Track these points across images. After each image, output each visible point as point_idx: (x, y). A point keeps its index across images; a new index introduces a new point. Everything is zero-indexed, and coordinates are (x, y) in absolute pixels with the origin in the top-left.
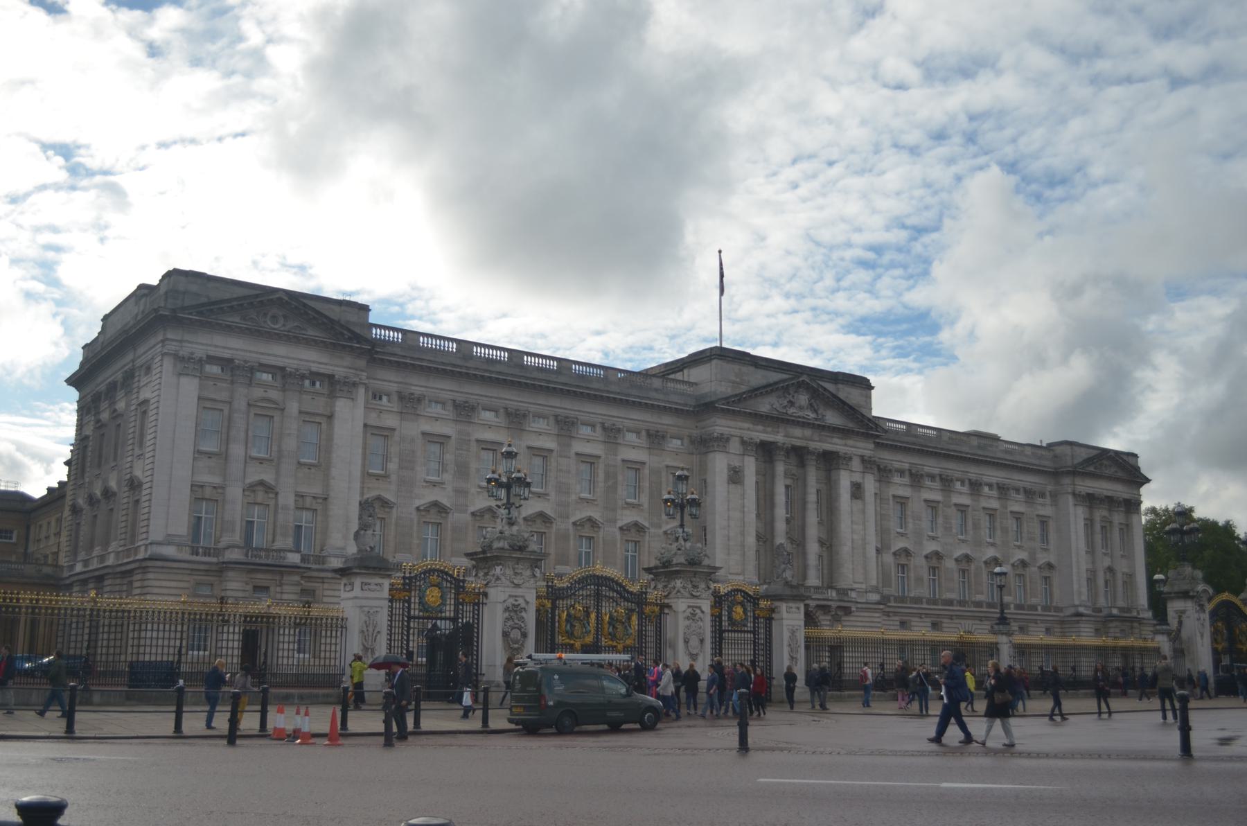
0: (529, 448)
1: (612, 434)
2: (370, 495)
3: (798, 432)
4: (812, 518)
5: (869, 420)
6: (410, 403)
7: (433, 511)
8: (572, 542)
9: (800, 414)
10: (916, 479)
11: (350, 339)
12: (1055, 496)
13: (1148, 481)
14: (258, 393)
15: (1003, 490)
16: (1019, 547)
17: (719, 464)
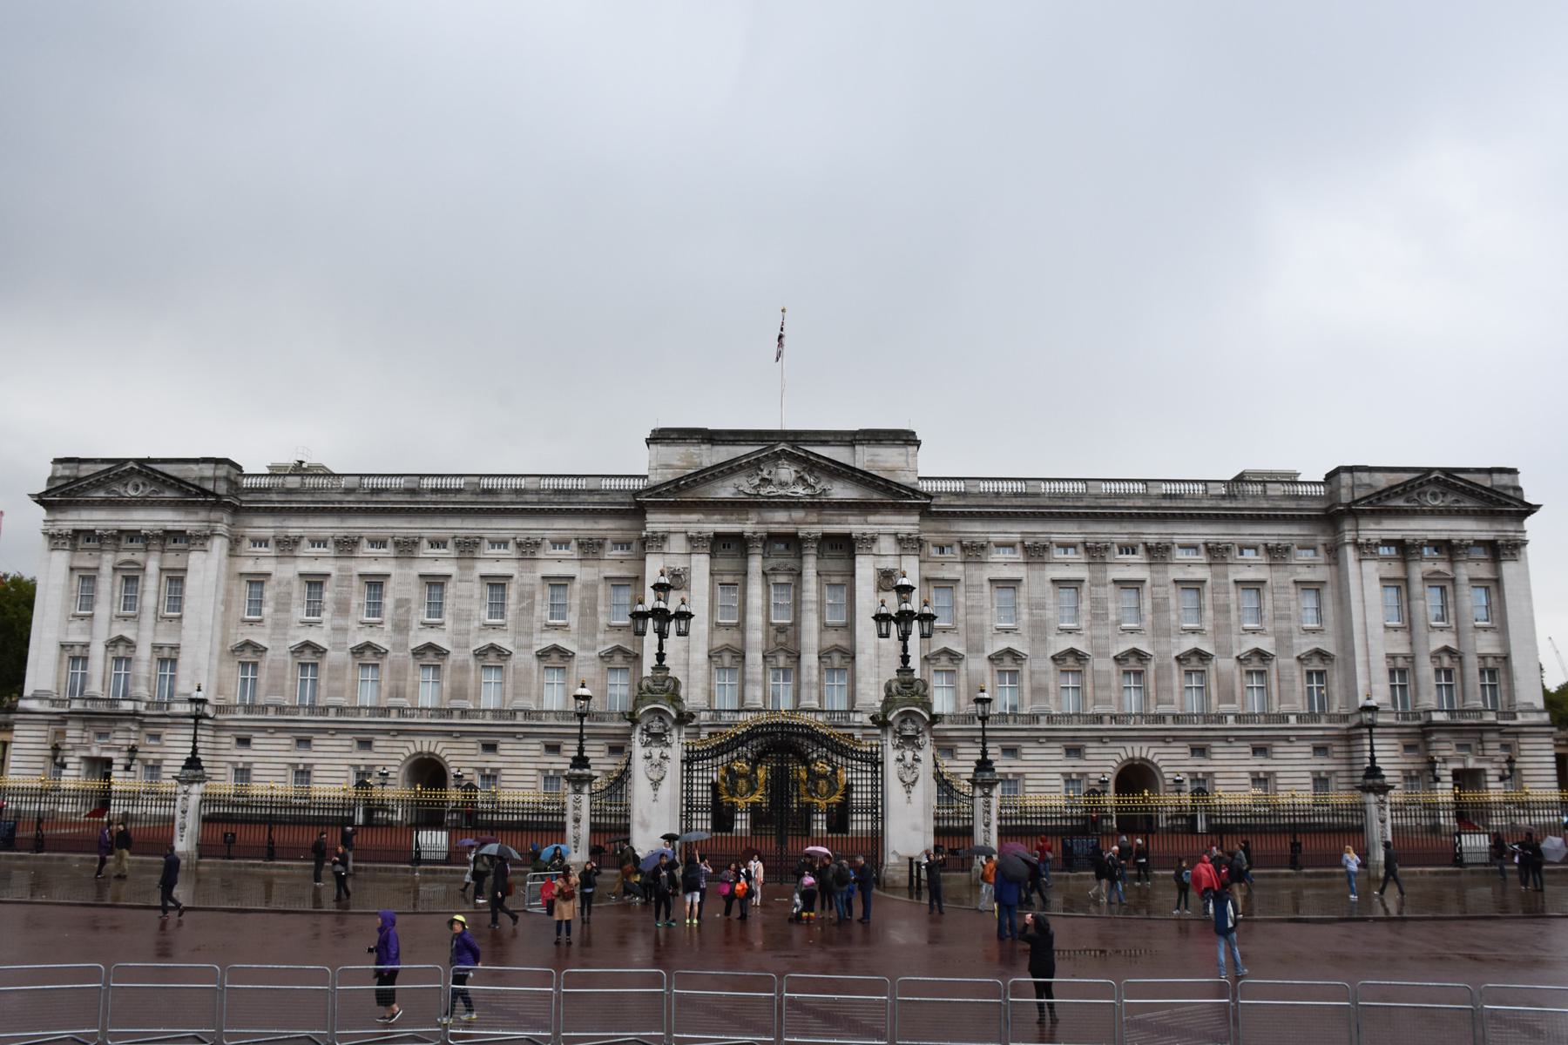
0: (421, 576)
1: (529, 549)
2: (241, 639)
3: (781, 516)
4: (810, 623)
5: (899, 485)
6: (288, 546)
7: (308, 652)
8: (472, 674)
9: (782, 492)
10: (1035, 553)
11: (197, 495)
12: (1334, 553)
13: (1539, 506)
14: (126, 556)
15: (1217, 553)
16: (1254, 631)
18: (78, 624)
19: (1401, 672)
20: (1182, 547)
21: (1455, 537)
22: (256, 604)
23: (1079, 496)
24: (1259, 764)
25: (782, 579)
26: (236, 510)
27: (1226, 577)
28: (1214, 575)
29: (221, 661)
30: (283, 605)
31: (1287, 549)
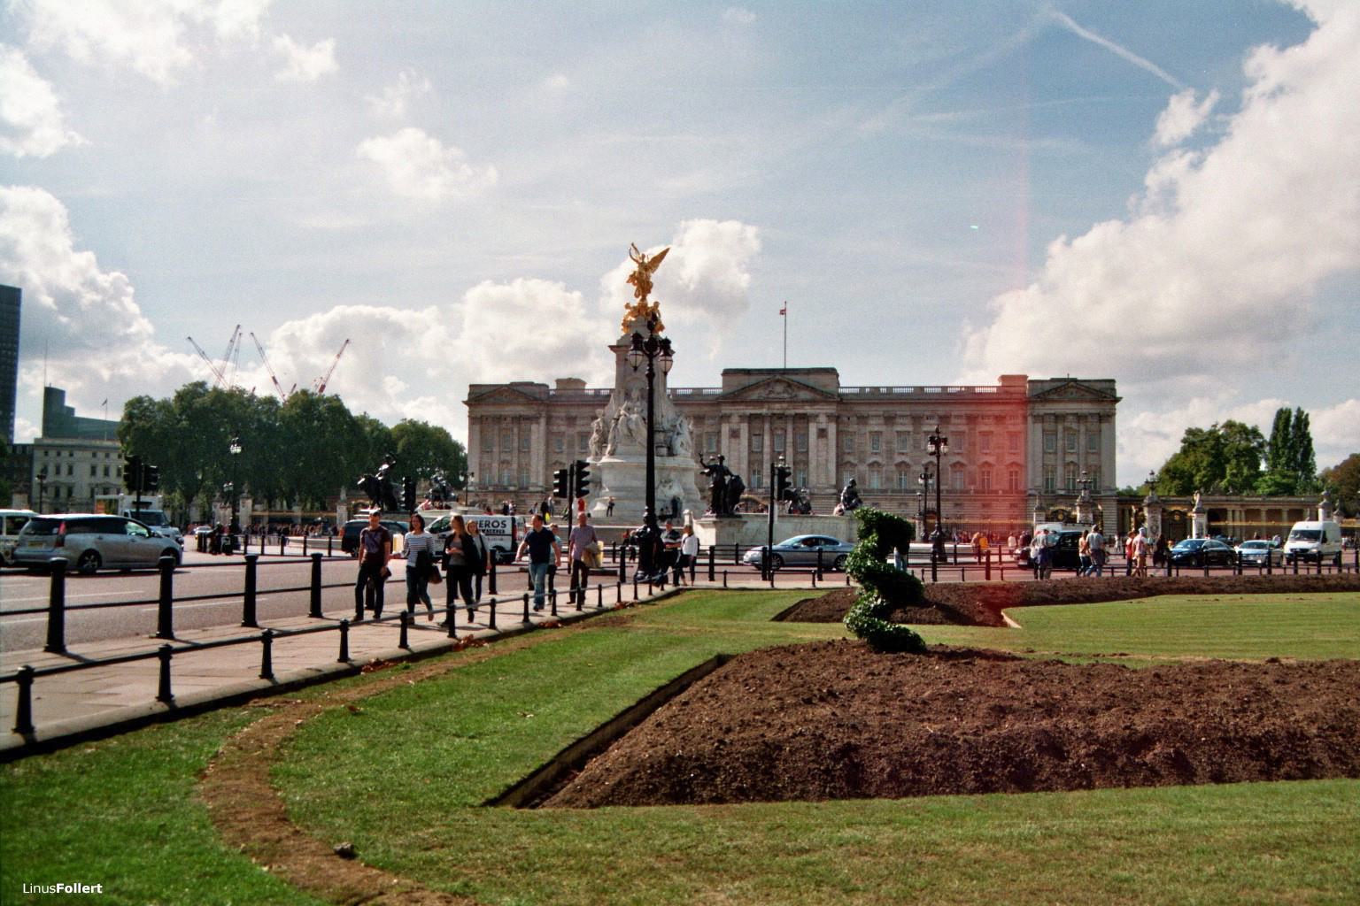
3: (777, 406)
10: (889, 420)
15: (972, 419)
16: (986, 454)
17: (725, 428)
18: (485, 455)
19: (1048, 470)
20: (956, 416)
21: (1079, 412)
22: (560, 443)
23: (908, 394)
24: (982, 511)
25: (779, 432)
26: (548, 405)
27: (974, 429)
28: (970, 429)
29: (547, 469)
30: (571, 445)
31: (1004, 417)
